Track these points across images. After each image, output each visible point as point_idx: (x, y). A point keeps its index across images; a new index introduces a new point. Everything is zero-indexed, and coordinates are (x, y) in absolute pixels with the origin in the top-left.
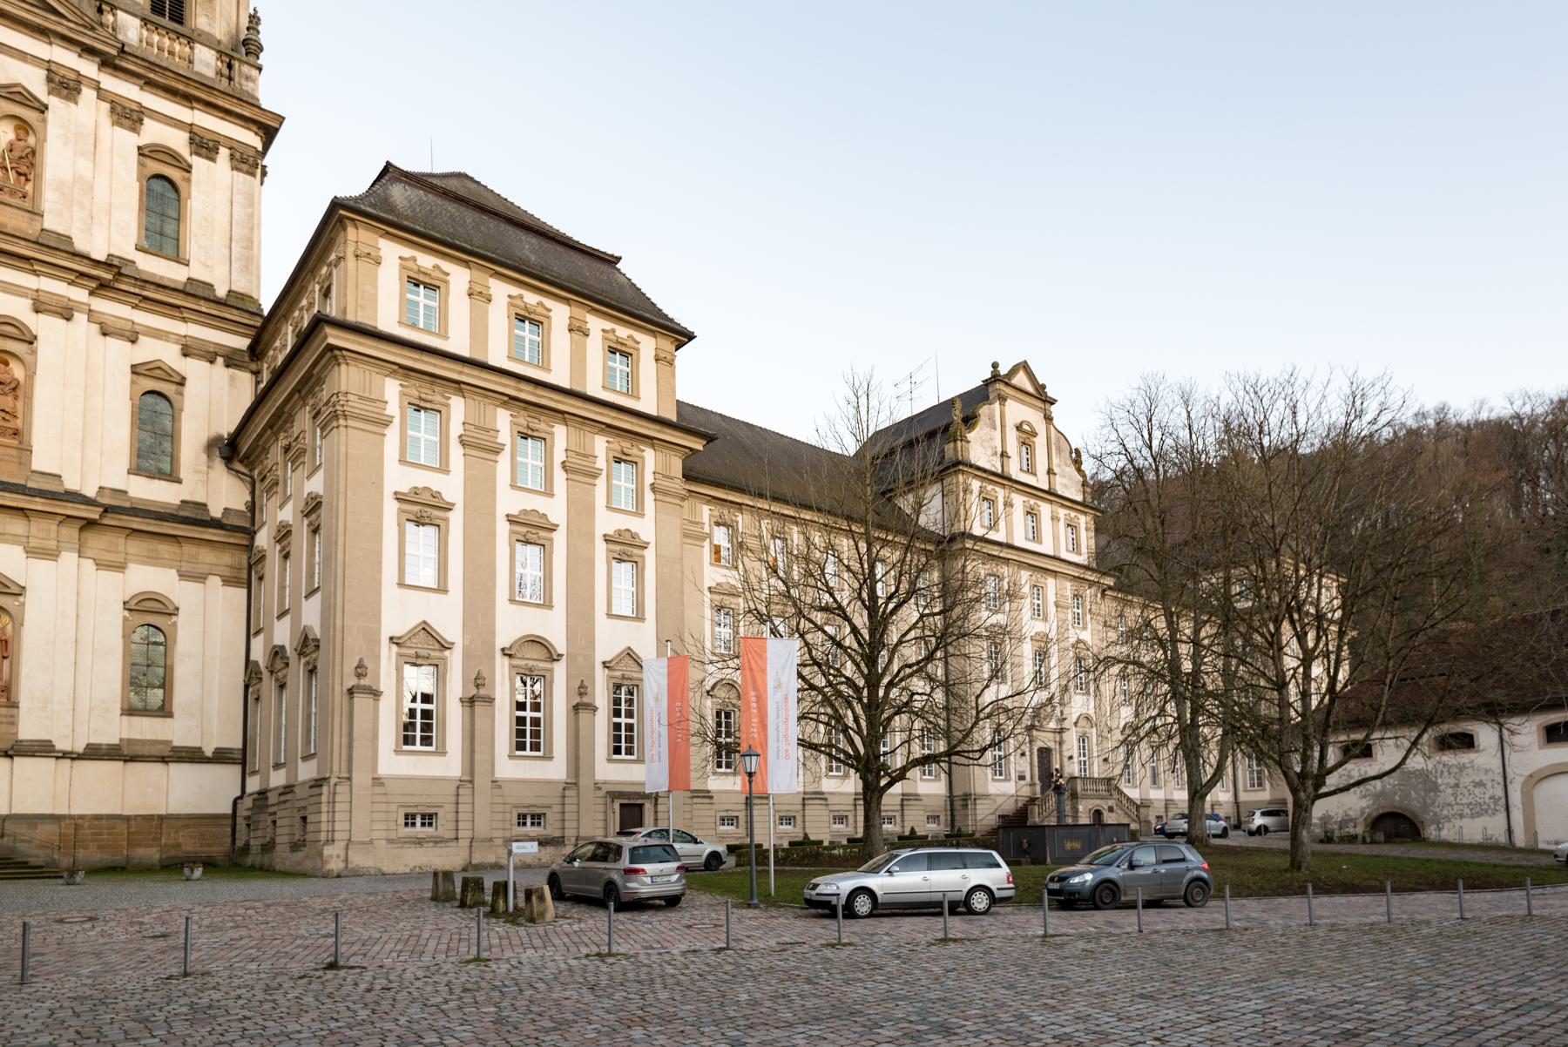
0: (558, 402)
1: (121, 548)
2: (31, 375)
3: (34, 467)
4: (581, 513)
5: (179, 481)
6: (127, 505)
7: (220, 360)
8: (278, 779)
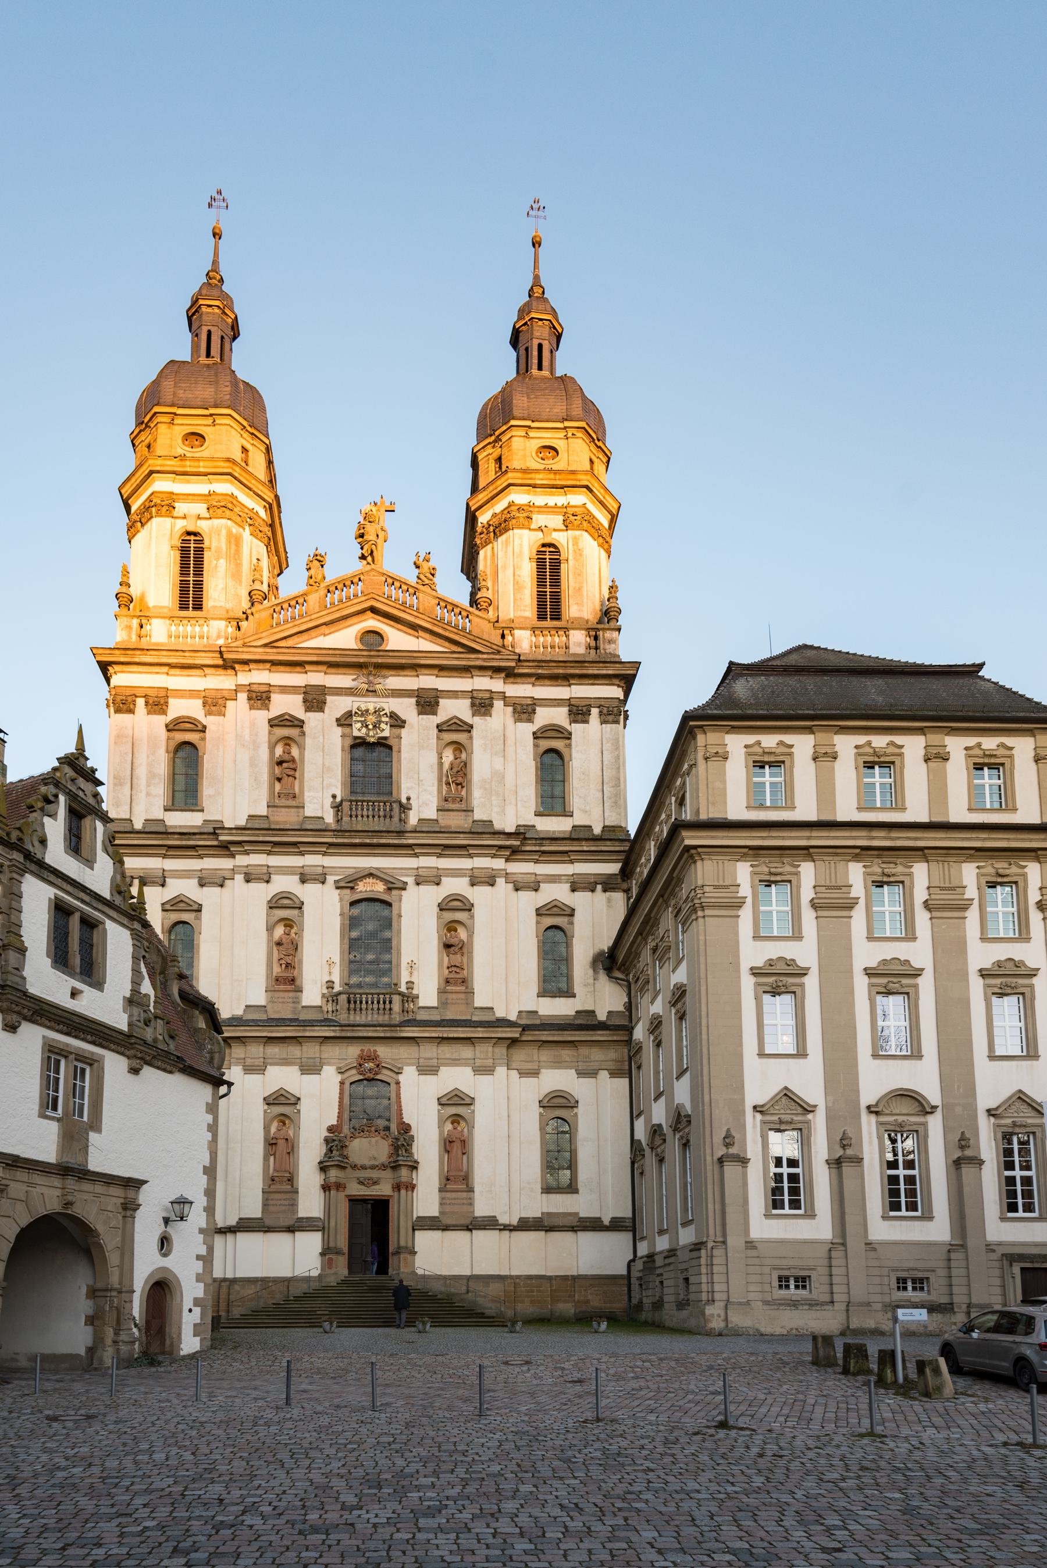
1: (535, 1058)
2: (471, 935)
3: (476, 1005)
6: (538, 1022)
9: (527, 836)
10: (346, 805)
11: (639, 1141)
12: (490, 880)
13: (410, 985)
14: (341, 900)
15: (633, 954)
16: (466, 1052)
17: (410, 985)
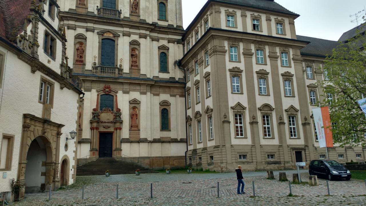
0: (267, 39)
2: (139, 53)
3: (141, 73)
4: (275, 68)
5: (169, 73)
7: (176, 43)
8: (200, 146)
9: (156, 26)
10: (102, 10)
11: (189, 116)
12: (145, 37)
13: (120, 66)
14: (99, 38)
15: (188, 62)
16: (138, 88)
17: (120, 66)
